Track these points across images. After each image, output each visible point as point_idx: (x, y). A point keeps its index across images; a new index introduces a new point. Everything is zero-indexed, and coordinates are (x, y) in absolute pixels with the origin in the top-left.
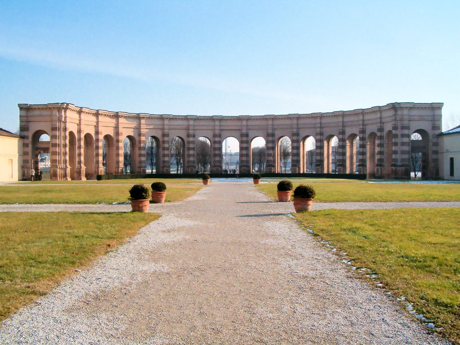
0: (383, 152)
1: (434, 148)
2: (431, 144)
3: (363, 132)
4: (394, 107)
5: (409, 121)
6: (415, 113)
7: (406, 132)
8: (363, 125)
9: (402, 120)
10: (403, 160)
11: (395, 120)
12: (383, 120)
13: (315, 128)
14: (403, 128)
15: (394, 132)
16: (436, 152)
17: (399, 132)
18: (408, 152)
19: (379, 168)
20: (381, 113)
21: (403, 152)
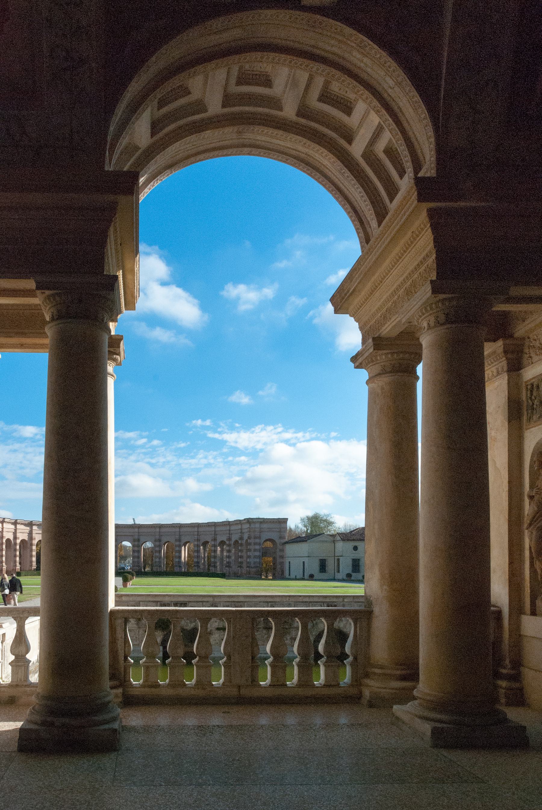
0: (243, 556)
1: (281, 554)
2: (278, 550)
3: (229, 539)
4: (249, 521)
5: (260, 532)
6: (265, 526)
7: (257, 541)
8: (229, 534)
9: (255, 531)
10: (255, 563)
11: (249, 532)
12: (243, 531)
13: (194, 535)
14: (255, 538)
15: (248, 540)
16: (282, 557)
17: (252, 541)
18: (259, 557)
19: (239, 568)
20: (241, 525)
21: (255, 557)
